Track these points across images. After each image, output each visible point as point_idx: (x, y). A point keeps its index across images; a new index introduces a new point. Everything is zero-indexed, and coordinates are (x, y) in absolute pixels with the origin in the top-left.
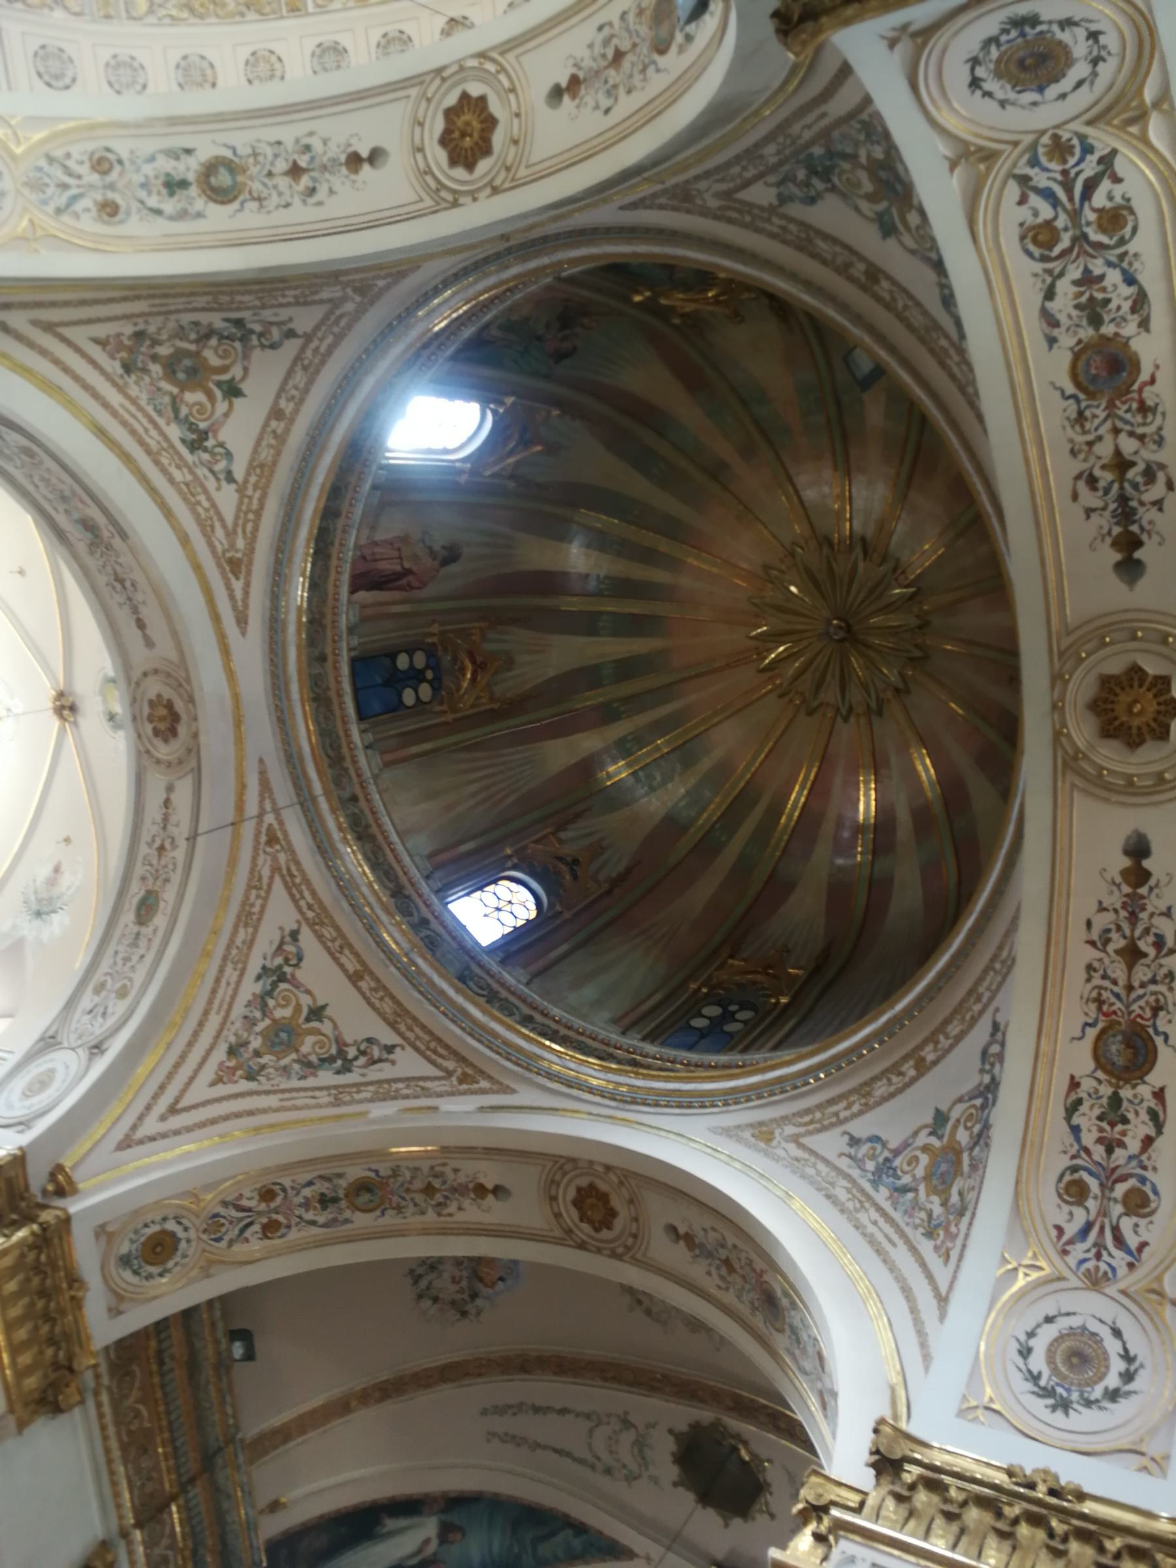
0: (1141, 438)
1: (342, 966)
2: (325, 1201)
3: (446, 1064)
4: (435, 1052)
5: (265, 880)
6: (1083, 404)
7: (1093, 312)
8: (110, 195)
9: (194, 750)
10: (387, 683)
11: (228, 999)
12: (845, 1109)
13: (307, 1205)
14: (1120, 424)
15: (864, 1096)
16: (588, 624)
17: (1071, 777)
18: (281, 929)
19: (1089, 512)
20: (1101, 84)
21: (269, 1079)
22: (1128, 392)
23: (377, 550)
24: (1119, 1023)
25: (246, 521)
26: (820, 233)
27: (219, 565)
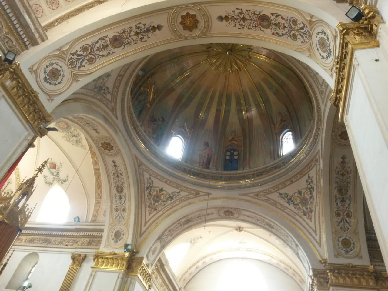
0: (130, 31)
1: (289, 185)
2: (343, 201)
3: (313, 165)
4: (310, 167)
5: (267, 198)
6: (125, 44)
7: (105, 47)
8: (122, 209)
9: (235, 209)
11: (292, 213)
13: (343, 206)
14: (128, 36)
16: (228, 112)
17: (208, 33)
18: (278, 197)
19: (148, 38)
20: (57, 61)
25: (188, 190)
26: (114, 85)
27: (196, 197)
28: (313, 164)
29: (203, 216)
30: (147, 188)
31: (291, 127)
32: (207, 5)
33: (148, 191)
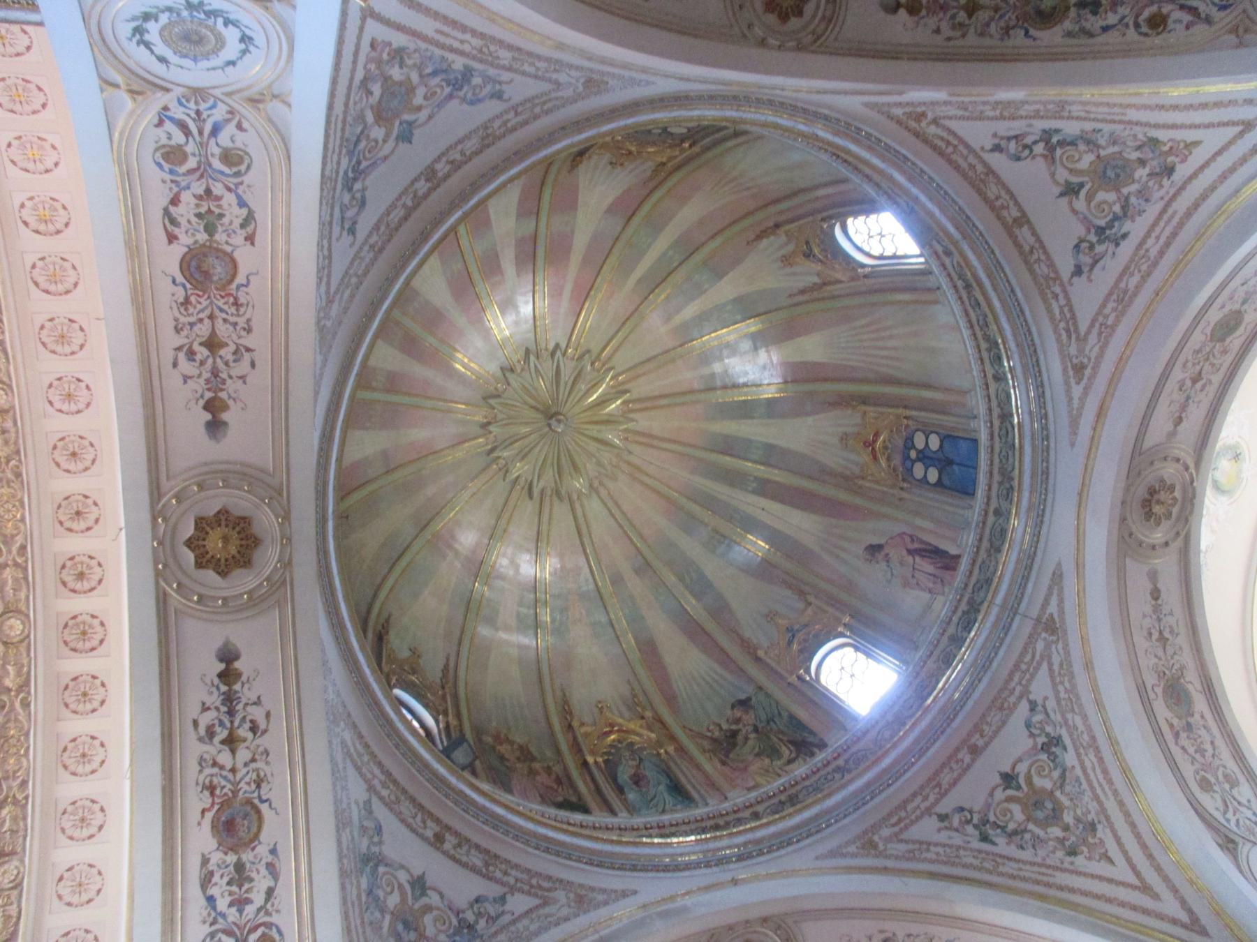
0: (215, 764)
1: (1034, 233)
3: (940, 132)
4: (948, 143)
5: (1095, 331)
6: (256, 794)
7: (240, 875)
10: (950, 462)
11: (1162, 224)
12: (508, 120)
14: (230, 776)
15: (488, 135)
16: (771, 454)
21: (1135, 136)
22: (222, 804)
23: (931, 585)
24: (217, 289)
28: (933, 129)
29: (1159, 620)
30: (985, 838)
31: (823, 220)
32: (163, 469)
33: (1001, 841)
